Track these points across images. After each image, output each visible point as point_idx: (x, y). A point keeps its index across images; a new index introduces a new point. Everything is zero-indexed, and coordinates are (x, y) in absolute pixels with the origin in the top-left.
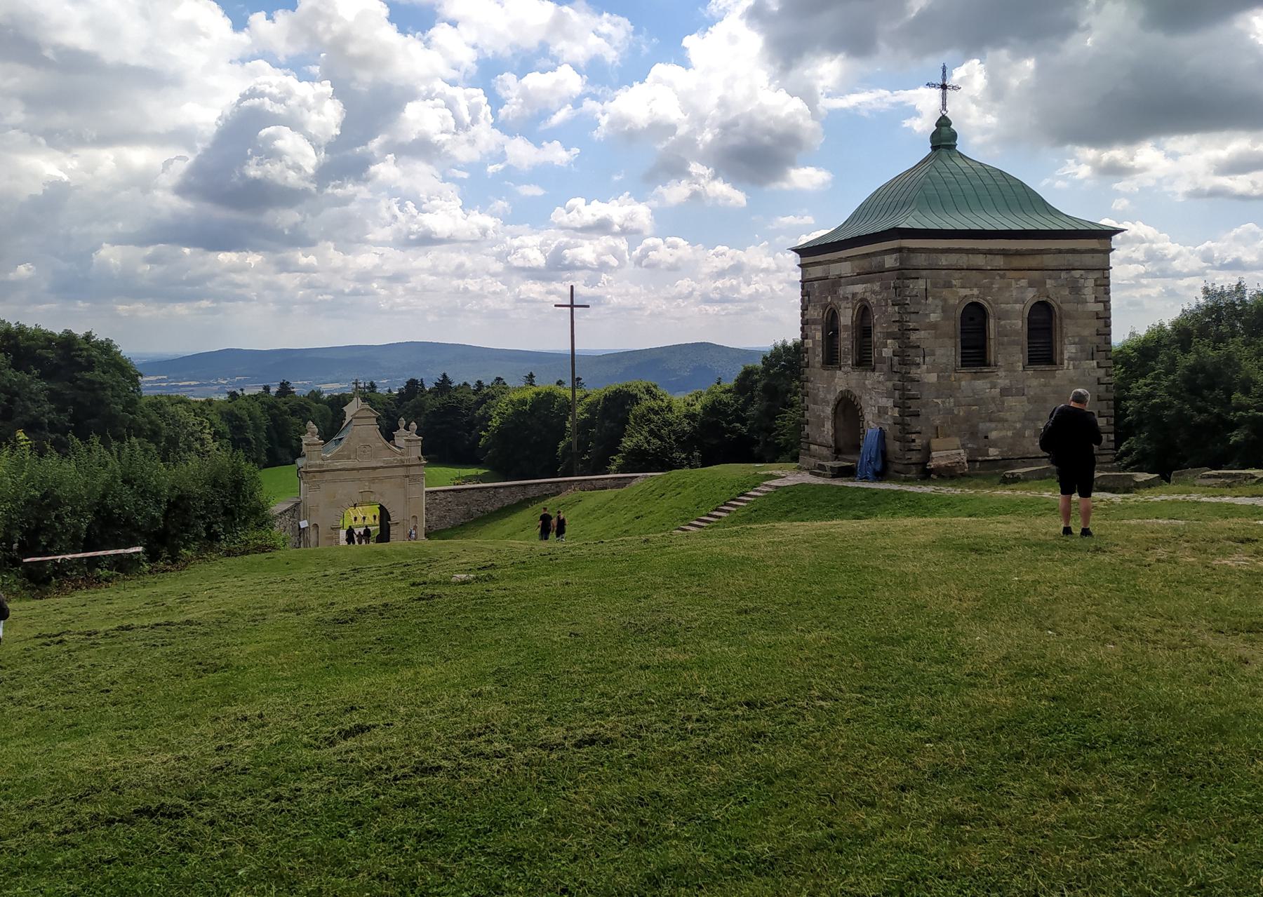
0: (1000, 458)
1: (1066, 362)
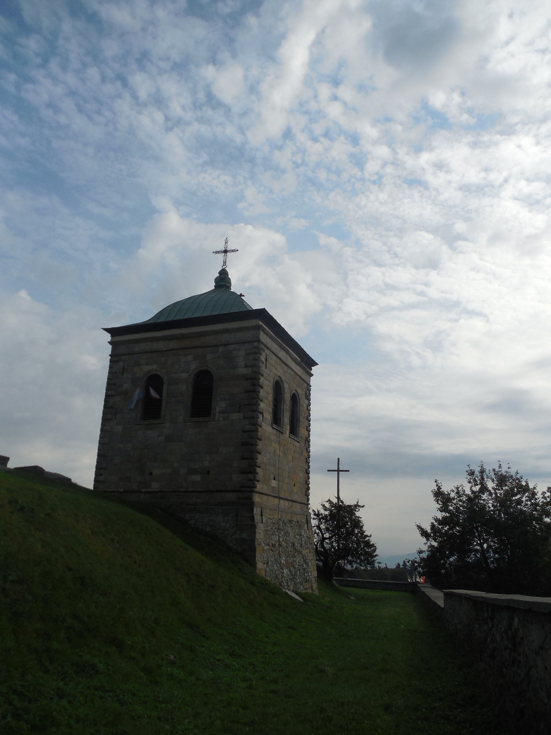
0: (158, 490)
1: (217, 414)
